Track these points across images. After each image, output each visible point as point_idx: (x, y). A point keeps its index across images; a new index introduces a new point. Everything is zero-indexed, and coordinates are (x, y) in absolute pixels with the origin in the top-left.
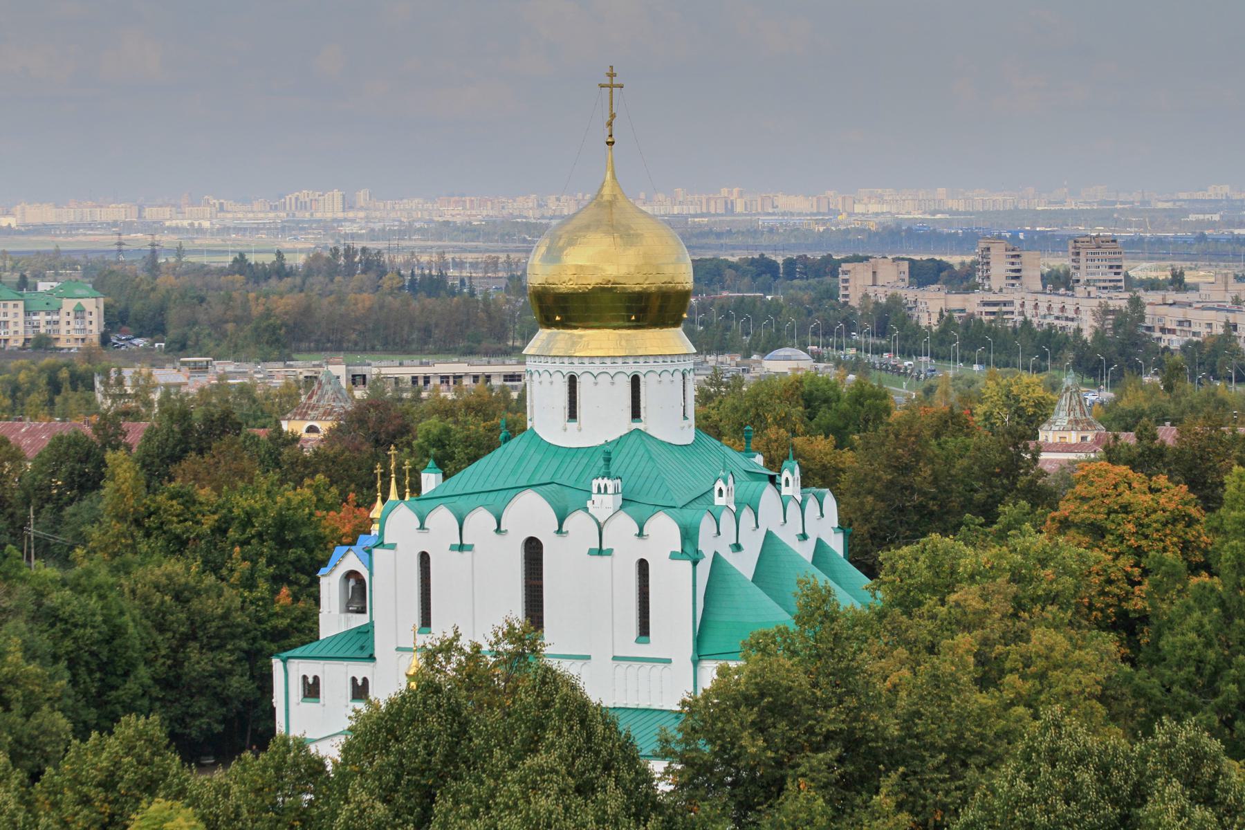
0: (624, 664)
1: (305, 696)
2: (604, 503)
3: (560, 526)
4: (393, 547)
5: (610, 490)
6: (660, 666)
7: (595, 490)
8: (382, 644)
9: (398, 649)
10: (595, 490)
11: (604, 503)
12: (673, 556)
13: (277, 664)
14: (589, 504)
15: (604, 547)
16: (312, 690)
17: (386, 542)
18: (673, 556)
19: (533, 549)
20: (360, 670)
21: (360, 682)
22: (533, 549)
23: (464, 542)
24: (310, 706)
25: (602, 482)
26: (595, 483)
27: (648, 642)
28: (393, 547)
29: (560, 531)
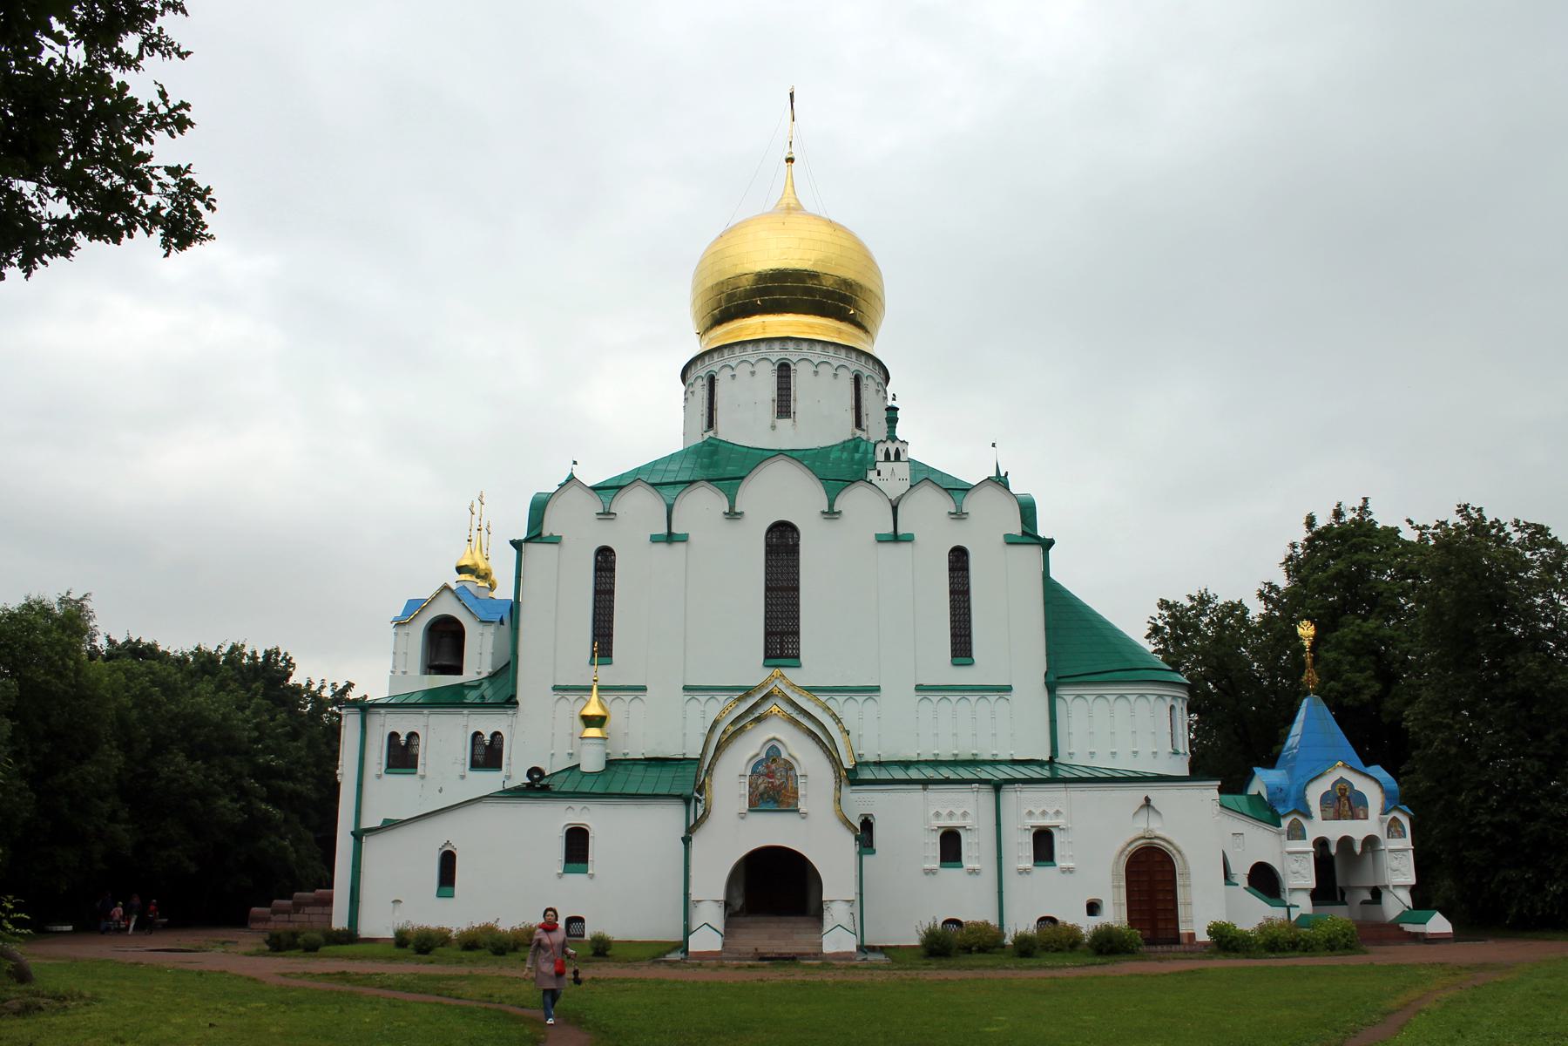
0: (935, 697)
1: (389, 766)
3: (831, 506)
4: (555, 540)
6: (993, 697)
7: (880, 456)
8: (531, 683)
9: (555, 688)
14: (872, 475)
15: (900, 531)
16: (402, 756)
17: (546, 533)
19: (782, 543)
20: (487, 724)
22: (782, 543)
23: (674, 530)
24: (400, 781)
27: (971, 664)
29: (831, 513)
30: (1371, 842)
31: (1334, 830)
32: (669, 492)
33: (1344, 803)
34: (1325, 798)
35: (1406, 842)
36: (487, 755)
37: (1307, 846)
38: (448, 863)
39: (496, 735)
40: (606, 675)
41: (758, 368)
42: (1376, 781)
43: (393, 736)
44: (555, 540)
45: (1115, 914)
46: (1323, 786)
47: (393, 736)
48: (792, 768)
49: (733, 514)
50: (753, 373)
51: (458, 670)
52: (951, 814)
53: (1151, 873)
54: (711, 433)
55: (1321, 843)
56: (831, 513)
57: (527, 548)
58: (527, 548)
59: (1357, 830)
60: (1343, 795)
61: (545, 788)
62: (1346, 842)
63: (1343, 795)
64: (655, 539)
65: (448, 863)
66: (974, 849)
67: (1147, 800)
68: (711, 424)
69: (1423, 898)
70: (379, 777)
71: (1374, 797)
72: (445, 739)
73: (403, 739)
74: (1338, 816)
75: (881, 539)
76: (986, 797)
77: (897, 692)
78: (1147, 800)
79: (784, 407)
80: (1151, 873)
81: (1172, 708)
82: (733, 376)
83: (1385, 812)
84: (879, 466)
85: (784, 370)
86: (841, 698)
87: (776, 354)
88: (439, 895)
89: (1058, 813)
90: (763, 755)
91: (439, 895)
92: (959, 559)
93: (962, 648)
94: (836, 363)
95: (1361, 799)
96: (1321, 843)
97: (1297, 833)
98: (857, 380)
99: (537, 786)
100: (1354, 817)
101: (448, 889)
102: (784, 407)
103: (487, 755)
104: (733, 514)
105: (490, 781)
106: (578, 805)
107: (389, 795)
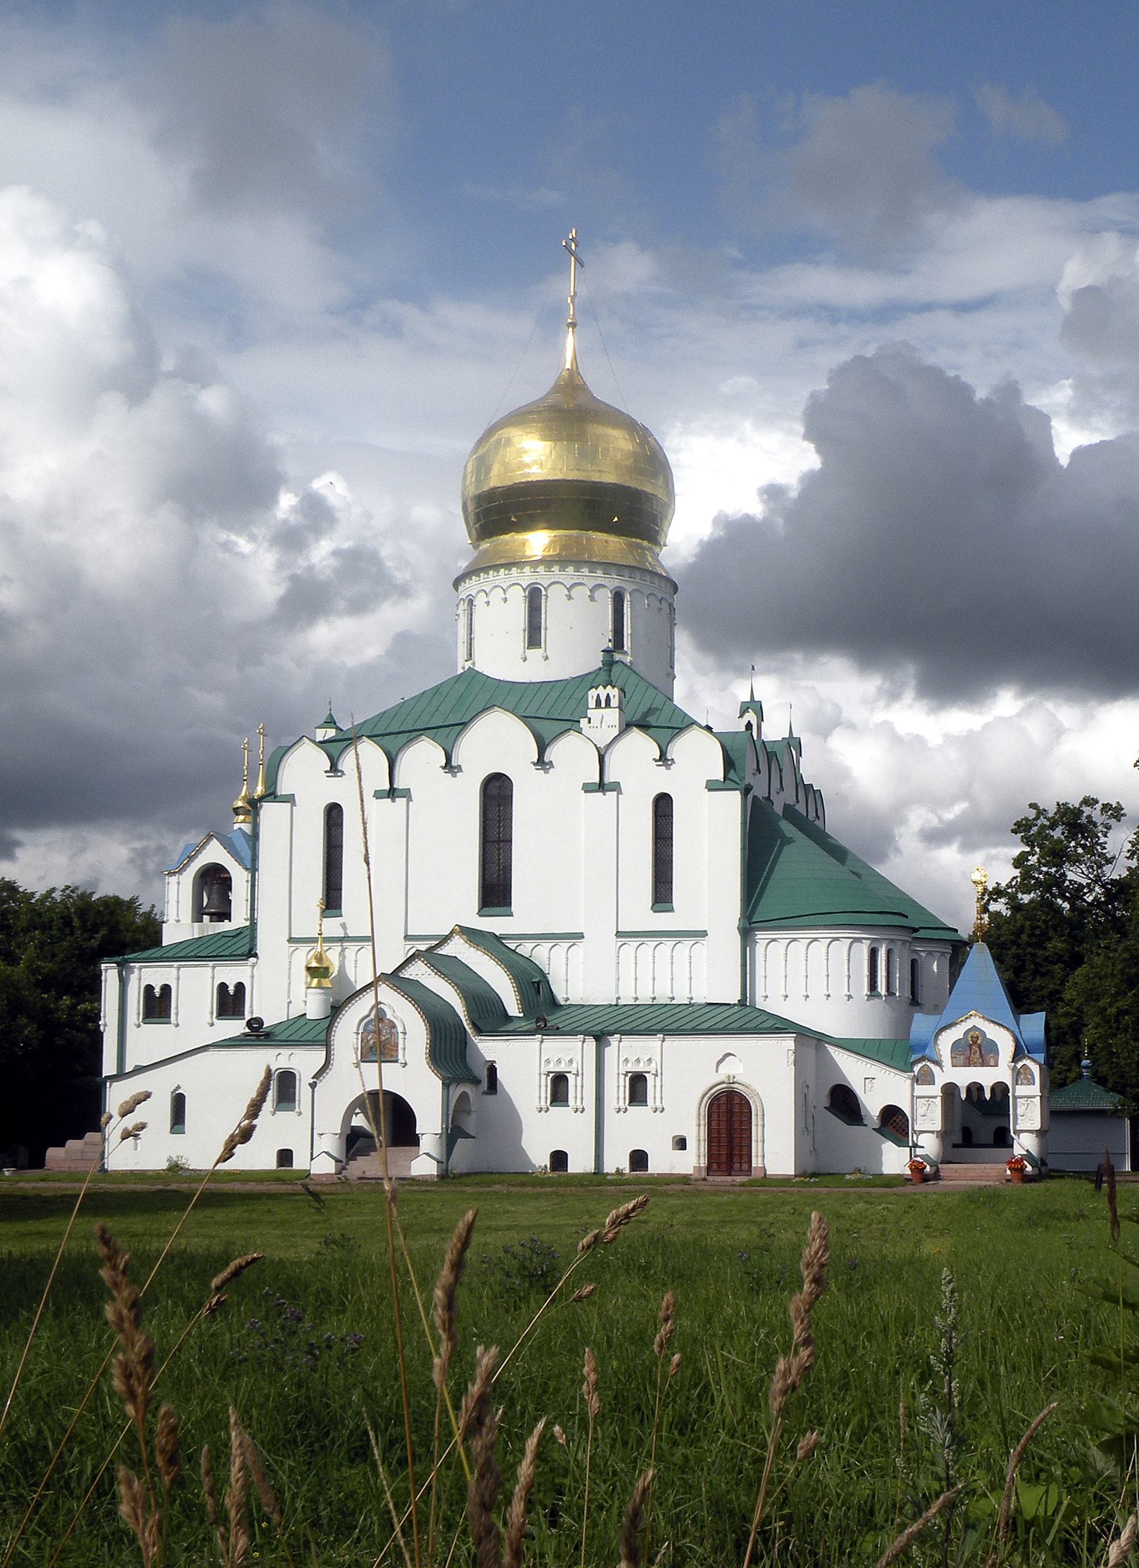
0: (633, 943)
2: (603, 722)
5: (615, 702)
6: (688, 942)
7: (592, 703)
8: (269, 940)
10: (592, 703)
11: (603, 722)
12: (712, 786)
13: (110, 975)
15: (606, 780)
16: (158, 1006)
18: (712, 786)
19: (496, 794)
20: (231, 974)
21: (231, 990)
22: (496, 794)
24: (156, 1030)
25: (602, 692)
26: (593, 693)
28: (290, 799)
29: (542, 763)
30: (1001, 1090)
31: (963, 1077)
32: (392, 742)
33: (976, 1050)
34: (956, 1046)
37: (936, 1090)
38: (179, 1103)
40: (332, 927)
42: (1008, 1029)
43: (149, 989)
46: (956, 1033)
47: (149, 989)
48: (394, 1026)
52: (559, 1061)
55: (950, 1090)
59: (986, 1077)
60: (975, 1043)
63: (975, 1043)
65: (179, 1103)
66: (581, 1090)
70: (139, 1026)
71: (1005, 1043)
74: (968, 1063)
75: (588, 788)
77: (600, 937)
81: (873, 953)
83: (1016, 1057)
84: (590, 713)
86: (547, 945)
88: (172, 1132)
90: (372, 1016)
91: (172, 1132)
92: (663, 806)
93: (662, 892)
94: (591, 583)
95: (993, 1048)
96: (950, 1090)
97: (926, 1078)
98: (618, 598)
99: (259, 1035)
100: (984, 1064)
102: (534, 637)
103: (230, 1002)
104: (449, 766)
105: (236, 1027)
106: (285, 1052)
107: (147, 1041)
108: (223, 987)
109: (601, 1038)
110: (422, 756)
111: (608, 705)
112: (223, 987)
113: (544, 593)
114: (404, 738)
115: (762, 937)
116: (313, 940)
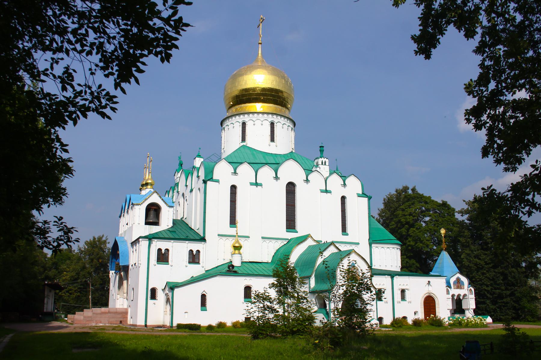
5: (327, 164)
7: (320, 163)
9: (219, 235)
10: (320, 163)
16: (163, 257)
17: (214, 178)
20: (195, 246)
22: (291, 188)
25: (324, 160)
29: (307, 181)
30: (465, 295)
35: (473, 296)
36: (194, 258)
38: (203, 297)
39: (198, 251)
41: (263, 123)
43: (160, 250)
44: (217, 181)
45: (421, 316)
47: (160, 250)
49: (277, 178)
50: (262, 125)
51: (156, 223)
53: (430, 303)
54: (244, 144)
55: (453, 296)
56: (307, 181)
57: (208, 182)
58: (208, 182)
59: (462, 292)
61: (235, 272)
62: (459, 295)
64: (252, 184)
65: (203, 297)
66: (387, 295)
67: (429, 282)
68: (243, 140)
69: (477, 312)
72: (179, 250)
73: (163, 251)
76: (388, 278)
78: (429, 282)
79: (272, 140)
80: (430, 303)
82: (254, 124)
85: (272, 124)
87: (270, 118)
89: (407, 285)
100: (461, 288)
101: (204, 308)
102: (272, 140)
103: (194, 258)
104: (277, 178)
106: (248, 278)
108: (191, 251)
109: (392, 277)
110: (266, 172)
111: (325, 164)
112: (191, 251)
113: (275, 124)
114: (261, 165)
115: (373, 245)
116: (234, 236)
